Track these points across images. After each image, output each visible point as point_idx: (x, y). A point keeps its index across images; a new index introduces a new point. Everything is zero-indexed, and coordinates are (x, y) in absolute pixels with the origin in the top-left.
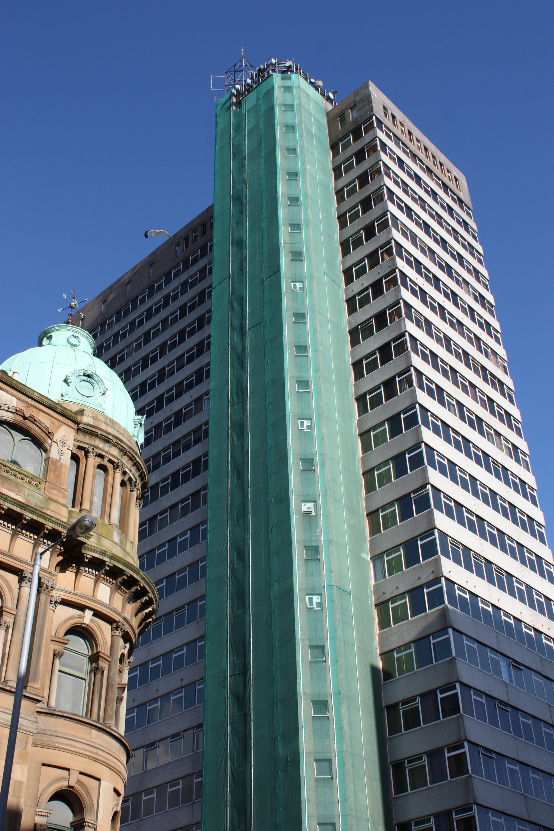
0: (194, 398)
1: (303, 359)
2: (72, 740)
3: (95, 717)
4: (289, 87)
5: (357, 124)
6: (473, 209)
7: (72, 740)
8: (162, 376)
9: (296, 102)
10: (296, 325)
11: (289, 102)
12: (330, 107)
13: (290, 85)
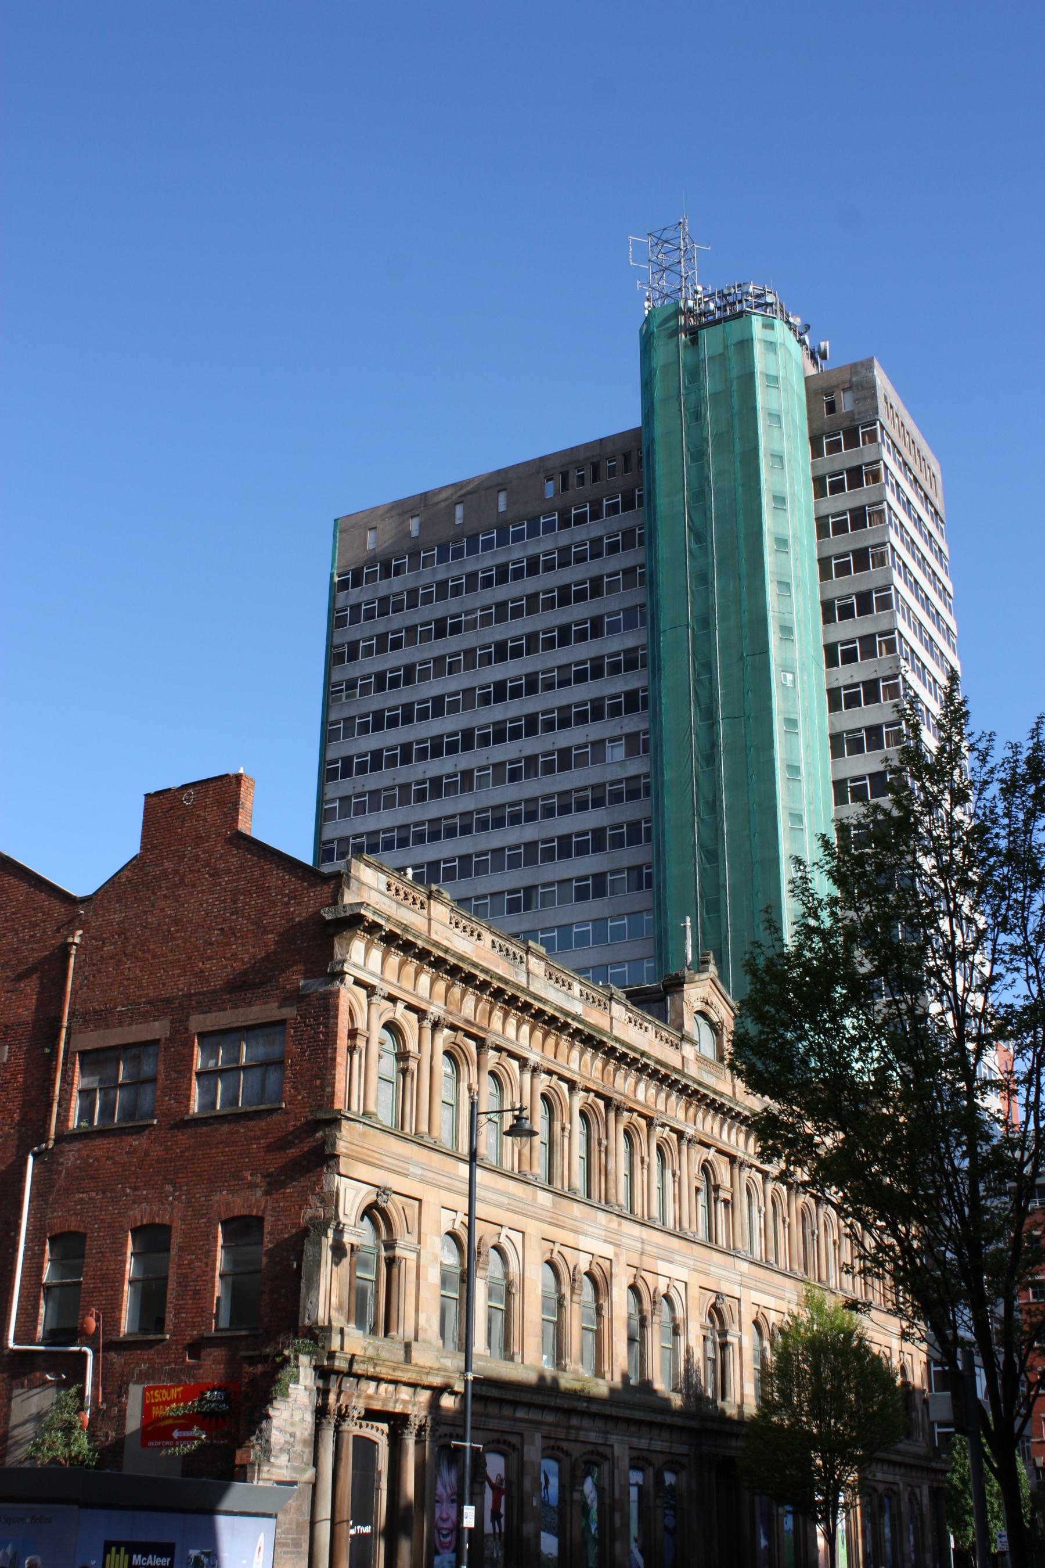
0: (591, 738)
1: (796, 784)
2: (741, 1372)
3: (407, 1130)
4: (771, 343)
5: (853, 423)
6: (947, 506)
7: (741, 1372)
8: (532, 684)
9: (781, 374)
10: (788, 736)
11: (773, 373)
12: (812, 371)
13: (773, 340)
